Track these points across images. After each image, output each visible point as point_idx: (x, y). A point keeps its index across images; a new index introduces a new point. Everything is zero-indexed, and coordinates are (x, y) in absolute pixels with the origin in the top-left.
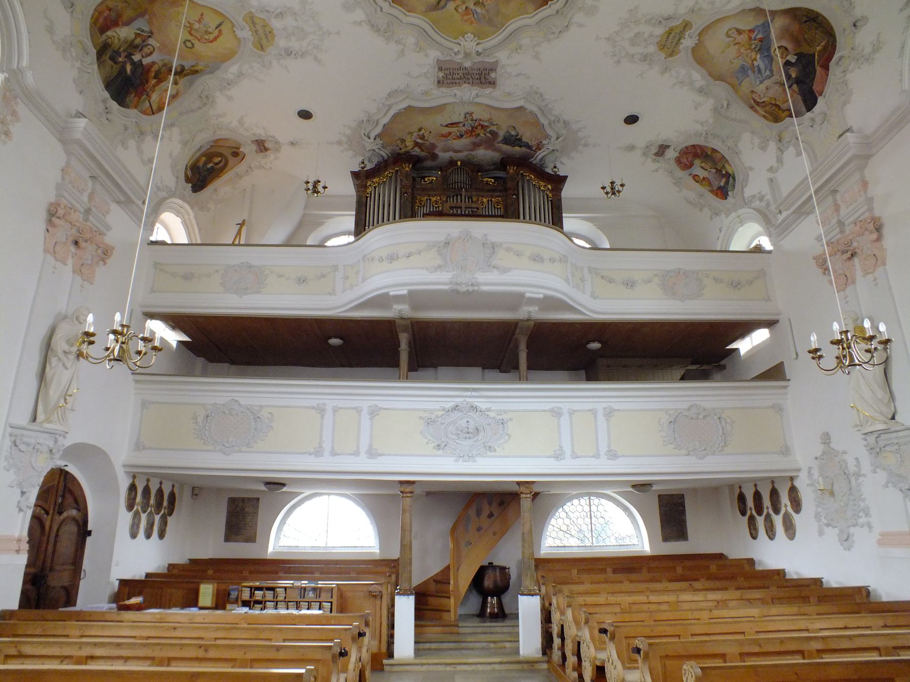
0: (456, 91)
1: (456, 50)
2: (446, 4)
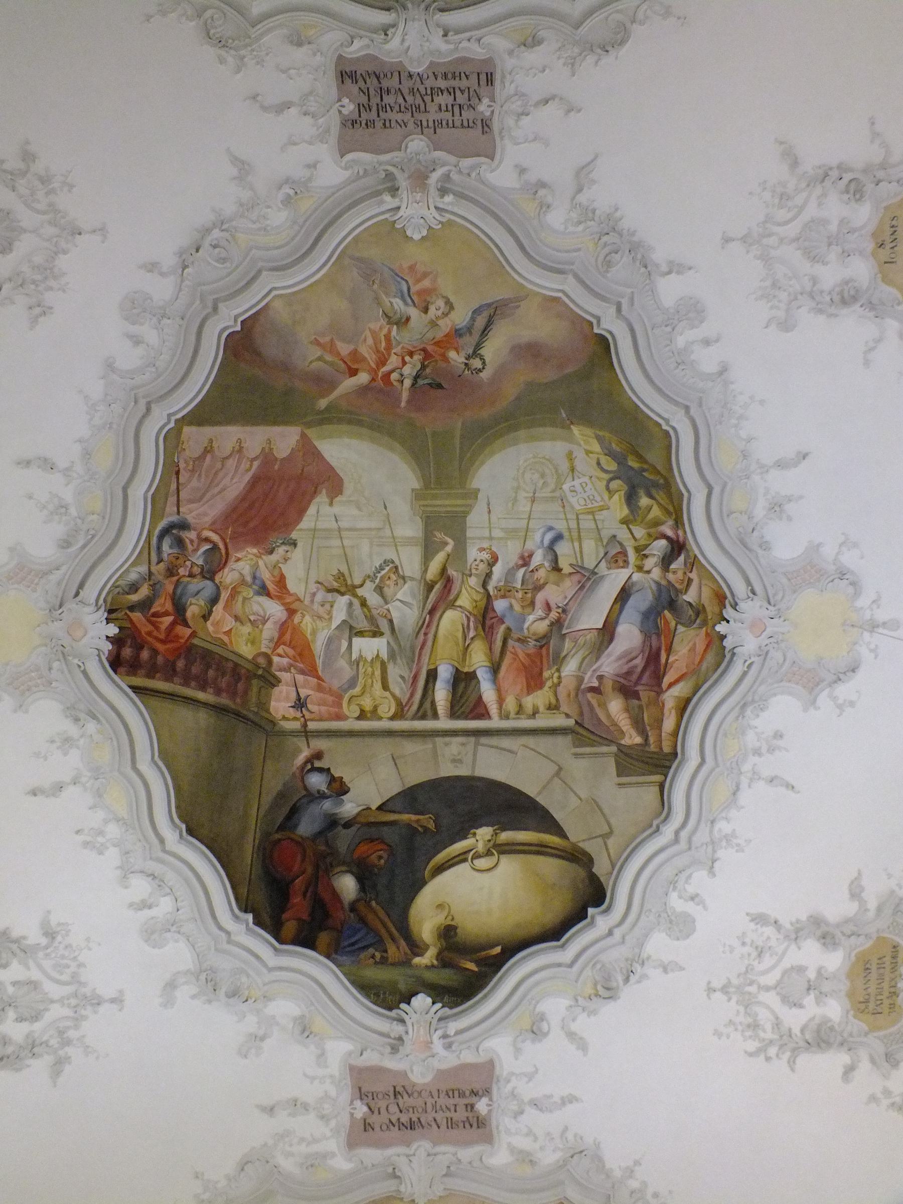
0: (444, 47)
1: (449, 198)
2: (473, 319)
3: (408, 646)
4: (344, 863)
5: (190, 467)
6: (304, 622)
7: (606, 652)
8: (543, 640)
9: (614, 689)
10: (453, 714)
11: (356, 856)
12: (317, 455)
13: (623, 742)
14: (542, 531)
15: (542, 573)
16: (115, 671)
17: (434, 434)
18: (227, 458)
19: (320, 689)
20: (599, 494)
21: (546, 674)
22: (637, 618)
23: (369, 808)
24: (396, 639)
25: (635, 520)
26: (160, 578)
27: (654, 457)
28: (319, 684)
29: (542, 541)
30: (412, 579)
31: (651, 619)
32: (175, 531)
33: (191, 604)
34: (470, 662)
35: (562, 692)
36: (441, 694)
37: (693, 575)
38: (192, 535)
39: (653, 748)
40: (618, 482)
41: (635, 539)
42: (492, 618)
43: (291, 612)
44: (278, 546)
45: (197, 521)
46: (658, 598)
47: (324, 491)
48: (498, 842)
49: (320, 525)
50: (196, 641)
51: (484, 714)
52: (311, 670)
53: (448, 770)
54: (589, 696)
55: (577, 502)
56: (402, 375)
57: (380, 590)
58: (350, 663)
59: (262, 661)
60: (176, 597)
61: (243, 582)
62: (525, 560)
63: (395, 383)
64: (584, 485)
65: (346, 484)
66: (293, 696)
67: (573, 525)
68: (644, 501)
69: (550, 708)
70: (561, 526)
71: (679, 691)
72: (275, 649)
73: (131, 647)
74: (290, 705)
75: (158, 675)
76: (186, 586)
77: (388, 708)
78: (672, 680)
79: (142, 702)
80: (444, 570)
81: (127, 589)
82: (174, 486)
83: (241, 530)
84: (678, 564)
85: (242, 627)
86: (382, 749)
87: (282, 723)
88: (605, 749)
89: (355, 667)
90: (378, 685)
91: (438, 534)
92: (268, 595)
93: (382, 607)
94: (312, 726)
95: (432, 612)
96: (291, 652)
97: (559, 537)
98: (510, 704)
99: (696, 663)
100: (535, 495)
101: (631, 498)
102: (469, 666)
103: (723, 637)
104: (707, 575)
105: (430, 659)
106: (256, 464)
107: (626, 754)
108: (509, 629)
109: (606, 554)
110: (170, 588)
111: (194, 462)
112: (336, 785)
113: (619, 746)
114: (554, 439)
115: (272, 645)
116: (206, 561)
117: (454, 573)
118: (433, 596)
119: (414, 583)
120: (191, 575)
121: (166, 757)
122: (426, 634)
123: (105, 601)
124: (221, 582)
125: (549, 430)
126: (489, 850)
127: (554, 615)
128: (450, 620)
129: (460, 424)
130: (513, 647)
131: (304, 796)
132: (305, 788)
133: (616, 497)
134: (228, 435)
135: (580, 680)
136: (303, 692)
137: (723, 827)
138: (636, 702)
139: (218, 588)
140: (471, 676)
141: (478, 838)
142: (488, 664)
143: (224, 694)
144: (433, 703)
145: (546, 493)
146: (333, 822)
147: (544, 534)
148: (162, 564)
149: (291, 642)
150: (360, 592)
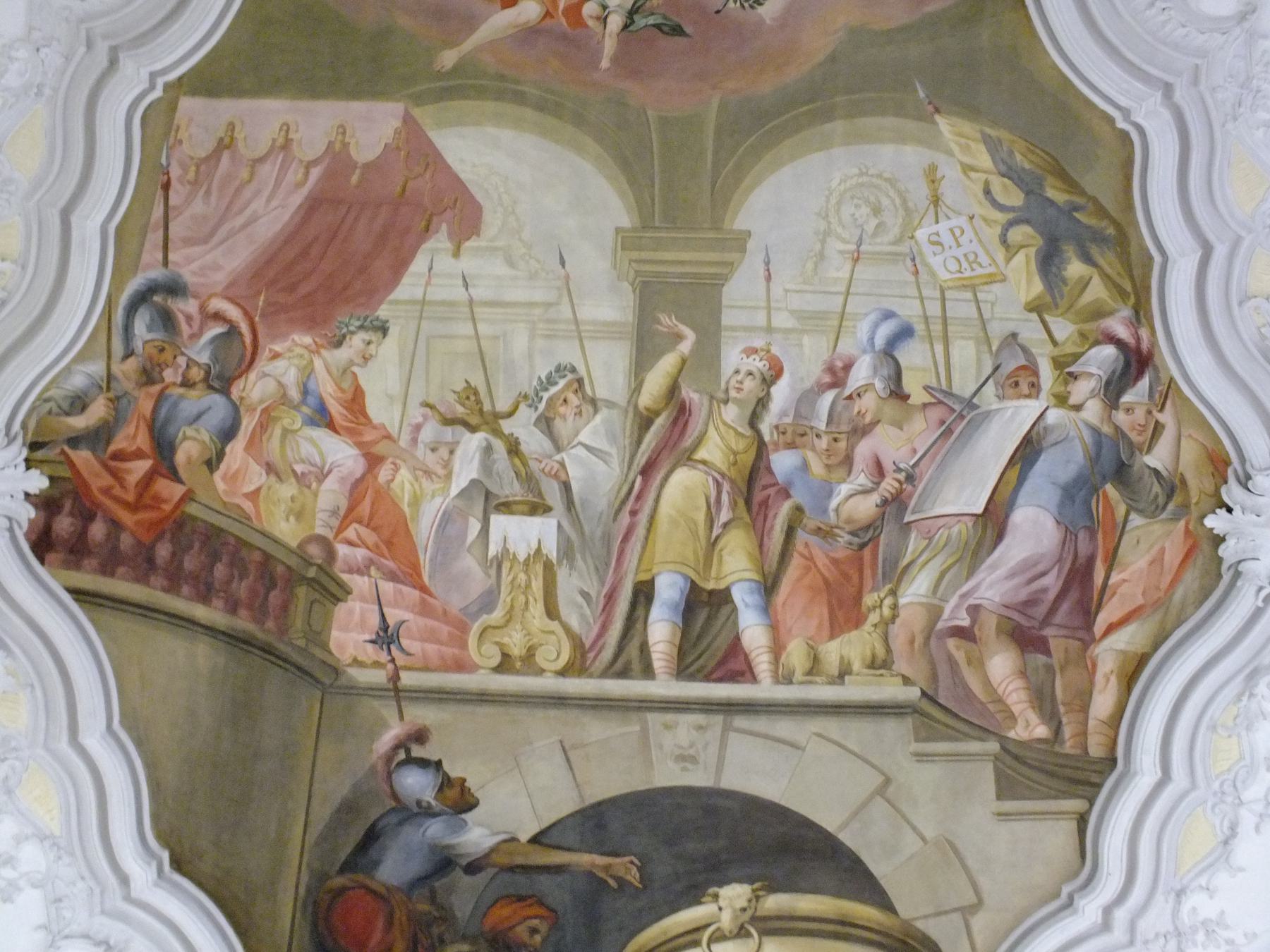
3: (599, 533)
4: (464, 938)
5: (191, 175)
6: (398, 479)
7: (990, 561)
8: (867, 534)
9: (999, 631)
10: (684, 668)
11: (487, 927)
12: (432, 159)
13: (1012, 734)
14: (873, 317)
15: (868, 403)
16: (42, 561)
17: (664, 122)
18: (261, 160)
19: (425, 610)
20: (988, 253)
21: (869, 599)
22: (1052, 496)
23: (514, 839)
24: (576, 522)
25: (1057, 306)
26: (129, 386)
27: (1098, 183)
28: (423, 601)
29: (871, 339)
30: (611, 404)
31: (1078, 499)
32: (159, 296)
33: (185, 438)
34: (719, 570)
35: (898, 634)
36: (661, 631)
37: (1166, 418)
38: (191, 306)
39: (1069, 747)
40: (1027, 229)
41: (1055, 343)
42: (765, 488)
43: (373, 461)
44: (352, 333)
45: (202, 280)
46: (1094, 459)
47: (444, 227)
48: (758, 914)
49: (436, 294)
50: (192, 509)
51: (745, 673)
52: (409, 574)
53: (668, 775)
54: (952, 643)
55: (942, 266)
56: (605, 7)
57: (546, 423)
58: (485, 562)
59: (314, 551)
60: (158, 424)
61: (284, 399)
62: (837, 375)
63: (590, 23)
64: (958, 233)
65: (487, 216)
66: (375, 621)
67: (934, 309)
68: (1075, 269)
69: (873, 664)
70: (909, 310)
71: (1126, 640)
72: (341, 530)
73: (71, 514)
74: (367, 637)
75: (121, 570)
76: (175, 405)
77: (554, 653)
78: (1114, 619)
79: (92, 621)
80: (673, 390)
81: (65, 406)
82: (158, 212)
83: (282, 298)
84: (1137, 394)
85: (281, 488)
86: (543, 730)
87: (354, 672)
88: (975, 746)
89: (493, 572)
90: (537, 609)
91: (664, 318)
92: (331, 426)
93: (550, 457)
94: (407, 679)
95: (647, 471)
96: (370, 537)
97: (905, 333)
98: (796, 655)
99: (1165, 584)
100: (860, 244)
101: (1048, 262)
102: (718, 579)
103: (1219, 540)
104: (1196, 418)
105: (640, 560)
106: (315, 173)
107: (1016, 758)
108: (799, 509)
109: (997, 368)
110: (147, 406)
111: (198, 166)
112: (452, 793)
113: (1003, 740)
114: (901, 139)
115: (335, 523)
116: (215, 358)
117: (695, 396)
118: (650, 440)
119: (615, 412)
120: (187, 384)
121: (135, 724)
122: (634, 513)
123: (24, 426)
124: (242, 398)
125: (889, 121)
126: (742, 927)
127: (889, 485)
128: (683, 488)
129: (715, 103)
130: (806, 545)
131: (393, 810)
132: (395, 796)
133: (1020, 258)
134: (264, 117)
135: (935, 613)
136: (393, 616)
137: (1199, 905)
138: (1041, 659)
139: (236, 409)
140: (722, 598)
141: (722, 903)
142: (756, 577)
143: (243, 612)
144: (644, 649)
145: (883, 244)
146: (444, 862)
147: (876, 326)
148: (131, 360)
149: (371, 519)
150: (507, 426)
